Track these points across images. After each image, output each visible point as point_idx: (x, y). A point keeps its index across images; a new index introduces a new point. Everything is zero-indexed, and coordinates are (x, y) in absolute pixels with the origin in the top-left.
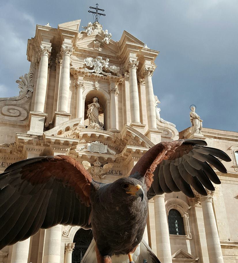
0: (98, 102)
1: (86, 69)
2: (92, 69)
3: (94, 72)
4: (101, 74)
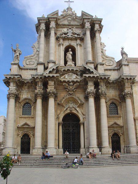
0: (72, 51)
1: (63, 35)
2: (67, 34)
4: (72, 36)
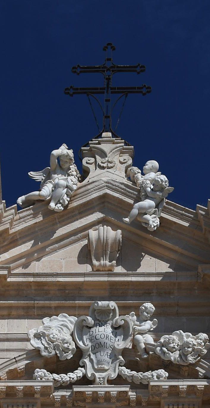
1: (40, 372)
3: (85, 381)
4: (119, 380)
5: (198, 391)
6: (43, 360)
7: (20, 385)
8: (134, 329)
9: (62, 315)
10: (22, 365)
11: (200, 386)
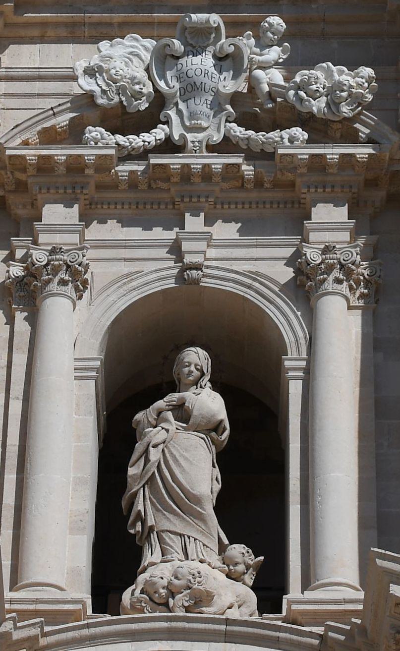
1: (94, 132)
3: (169, 146)
4: (226, 146)
5: (358, 164)
6: (99, 112)
7: (60, 153)
8: (251, 60)
9: (131, 37)
10: (63, 120)
11: (361, 156)
